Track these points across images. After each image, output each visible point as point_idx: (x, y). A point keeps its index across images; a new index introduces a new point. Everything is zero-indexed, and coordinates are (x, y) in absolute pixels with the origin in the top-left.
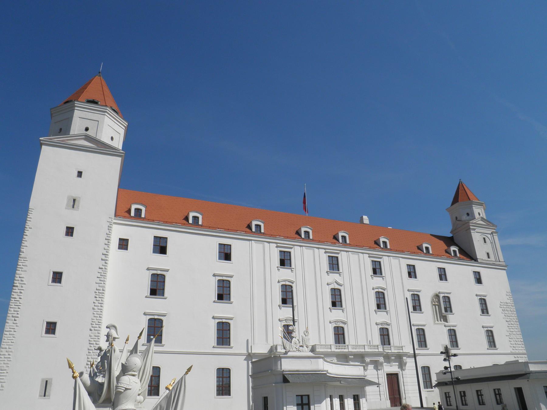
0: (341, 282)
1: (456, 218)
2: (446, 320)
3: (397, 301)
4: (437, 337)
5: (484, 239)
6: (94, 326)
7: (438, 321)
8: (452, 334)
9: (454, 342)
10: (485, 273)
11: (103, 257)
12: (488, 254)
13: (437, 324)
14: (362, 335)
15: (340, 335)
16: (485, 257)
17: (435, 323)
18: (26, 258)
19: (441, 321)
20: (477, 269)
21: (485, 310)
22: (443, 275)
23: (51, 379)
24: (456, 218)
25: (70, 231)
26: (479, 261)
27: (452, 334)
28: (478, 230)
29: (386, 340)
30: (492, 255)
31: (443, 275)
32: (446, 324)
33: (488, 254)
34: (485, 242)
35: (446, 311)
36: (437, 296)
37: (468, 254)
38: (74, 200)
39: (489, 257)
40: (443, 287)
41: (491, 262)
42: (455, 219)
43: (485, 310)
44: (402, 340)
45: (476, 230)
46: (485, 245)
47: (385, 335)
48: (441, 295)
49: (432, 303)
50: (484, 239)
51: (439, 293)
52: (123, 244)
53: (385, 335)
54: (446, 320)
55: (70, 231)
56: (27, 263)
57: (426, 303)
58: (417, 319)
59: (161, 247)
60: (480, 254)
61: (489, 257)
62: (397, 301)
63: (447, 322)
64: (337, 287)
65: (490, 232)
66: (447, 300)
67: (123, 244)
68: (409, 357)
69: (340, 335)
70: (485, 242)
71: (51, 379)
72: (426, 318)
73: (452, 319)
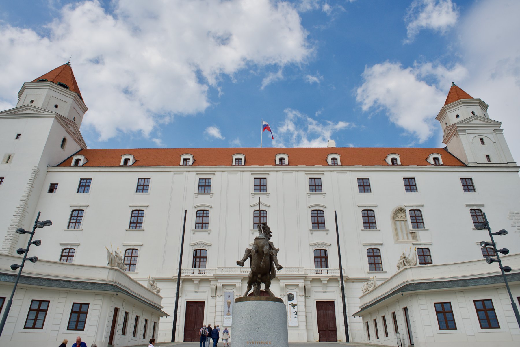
2: (415, 238)
7: (404, 239)
10: (478, 179)
12: (488, 156)
13: (401, 242)
16: (485, 160)
19: (408, 238)
22: (410, 185)
31: (410, 185)
32: (415, 242)
33: (488, 156)
36: (401, 210)
40: (410, 200)
45: (467, 131)
46: (483, 147)
48: (407, 210)
54: (415, 238)
63: (417, 240)
73: (424, 238)
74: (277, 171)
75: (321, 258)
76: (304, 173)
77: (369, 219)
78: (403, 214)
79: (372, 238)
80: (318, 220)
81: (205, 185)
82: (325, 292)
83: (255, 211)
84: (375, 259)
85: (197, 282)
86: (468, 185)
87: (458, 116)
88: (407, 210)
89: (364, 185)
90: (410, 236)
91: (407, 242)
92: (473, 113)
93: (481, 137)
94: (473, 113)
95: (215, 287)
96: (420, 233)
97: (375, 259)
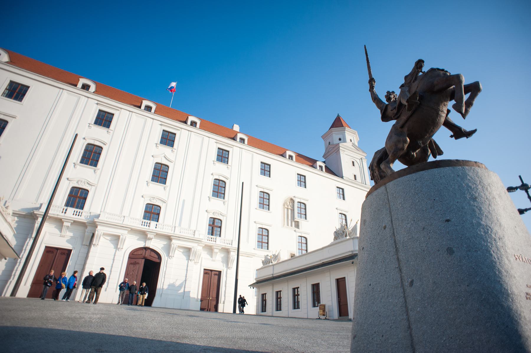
1: (329, 143)
5: (353, 162)
12: (355, 176)
16: (353, 178)
22: (302, 180)
24: (329, 143)
28: (347, 152)
30: (358, 177)
31: (302, 180)
32: (297, 229)
34: (353, 165)
37: (333, 169)
39: (355, 179)
40: (300, 194)
42: (328, 144)
45: (345, 153)
47: (215, 226)
48: (296, 200)
49: (284, 205)
50: (353, 162)
51: (294, 197)
54: (297, 225)
61: (355, 179)
64: (164, 162)
65: (359, 158)
66: (303, 206)
70: (353, 165)
72: (275, 218)
75: (215, 226)
77: (265, 200)
79: (263, 218)
80: (219, 189)
81: (104, 119)
83: (156, 163)
84: (264, 237)
85: (69, 224)
89: (266, 170)
93: (354, 161)
95: (91, 235)
97: (264, 237)
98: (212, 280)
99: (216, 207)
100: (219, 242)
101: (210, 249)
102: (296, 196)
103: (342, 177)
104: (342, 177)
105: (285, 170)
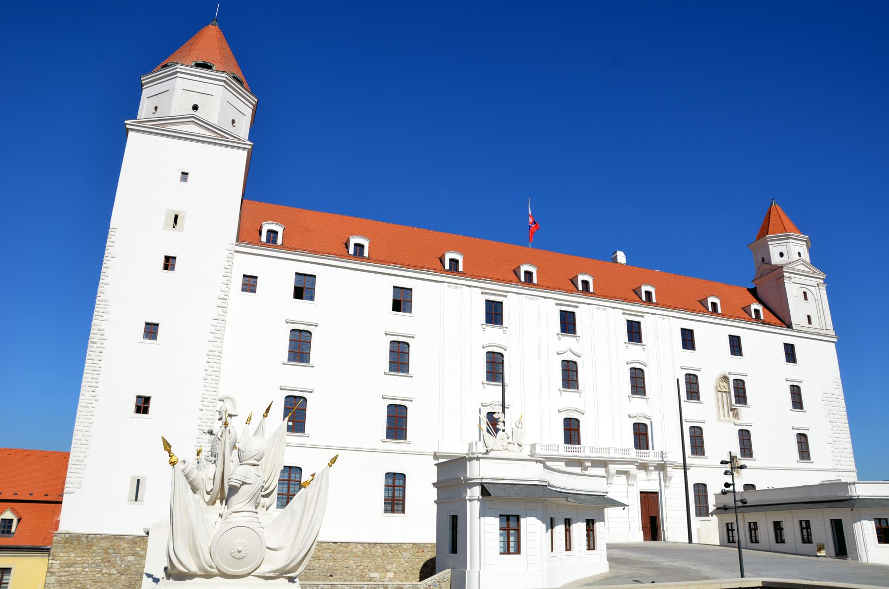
0: (578, 352)
1: (763, 259)
2: (736, 416)
3: (663, 383)
4: (721, 442)
5: (805, 293)
6: (206, 403)
8: (745, 437)
9: (746, 448)
11: (220, 303)
12: (809, 317)
13: (723, 421)
14: (608, 434)
15: (572, 431)
17: (719, 420)
18: (106, 301)
20: (790, 340)
21: (797, 402)
23: (145, 478)
24: (763, 259)
25: (169, 263)
26: (794, 327)
27: (745, 437)
28: (796, 279)
29: (643, 442)
32: (737, 421)
33: (809, 317)
34: (806, 299)
35: (738, 402)
36: (725, 378)
38: (176, 217)
39: (810, 322)
40: (735, 366)
41: (814, 331)
42: (760, 260)
43: (797, 402)
44: (667, 441)
45: (793, 280)
47: (641, 436)
48: (731, 378)
49: (717, 388)
50: (805, 293)
52: (250, 283)
53: (641, 436)
54: (736, 416)
55: (169, 263)
56: (108, 309)
57: (706, 387)
58: (693, 412)
59: (303, 289)
60: (797, 316)
61: (810, 322)
62: (663, 383)
67: (250, 283)
68: (676, 467)
69: (572, 431)
70: (806, 299)
71: (145, 478)
72: (707, 411)
73: (747, 415)
74: (589, 304)
76: (622, 311)
78: (725, 384)
82: (649, 480)
86: (790, 353)
87: (782, 255)
88: (731, 378)
90: (731, 413)
91: (729, 422)
92: (799, 254)
94: (799, 254)
96: (742, 409)
98: (650, 503)
99: (639, 408)
100: (651, 456)
101: (643, 467)
102: (732, 371)
103: (789, 326)
104: (789, 326)
105: (712, 334)
